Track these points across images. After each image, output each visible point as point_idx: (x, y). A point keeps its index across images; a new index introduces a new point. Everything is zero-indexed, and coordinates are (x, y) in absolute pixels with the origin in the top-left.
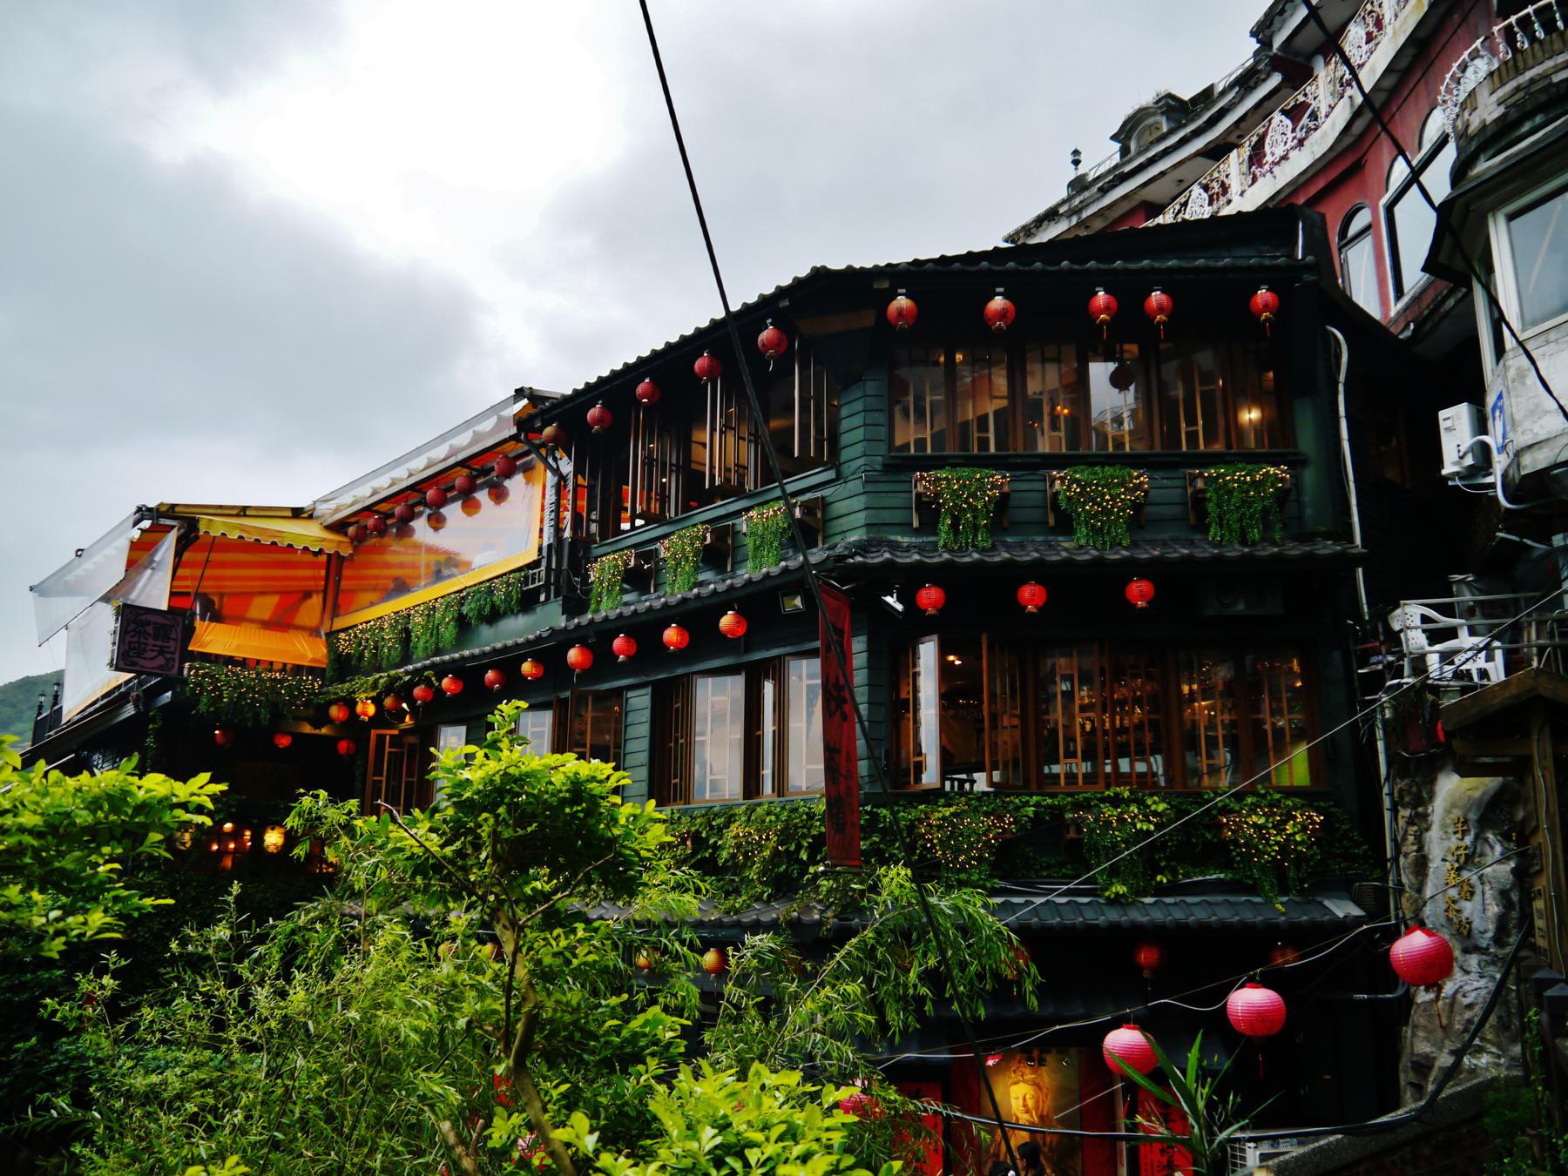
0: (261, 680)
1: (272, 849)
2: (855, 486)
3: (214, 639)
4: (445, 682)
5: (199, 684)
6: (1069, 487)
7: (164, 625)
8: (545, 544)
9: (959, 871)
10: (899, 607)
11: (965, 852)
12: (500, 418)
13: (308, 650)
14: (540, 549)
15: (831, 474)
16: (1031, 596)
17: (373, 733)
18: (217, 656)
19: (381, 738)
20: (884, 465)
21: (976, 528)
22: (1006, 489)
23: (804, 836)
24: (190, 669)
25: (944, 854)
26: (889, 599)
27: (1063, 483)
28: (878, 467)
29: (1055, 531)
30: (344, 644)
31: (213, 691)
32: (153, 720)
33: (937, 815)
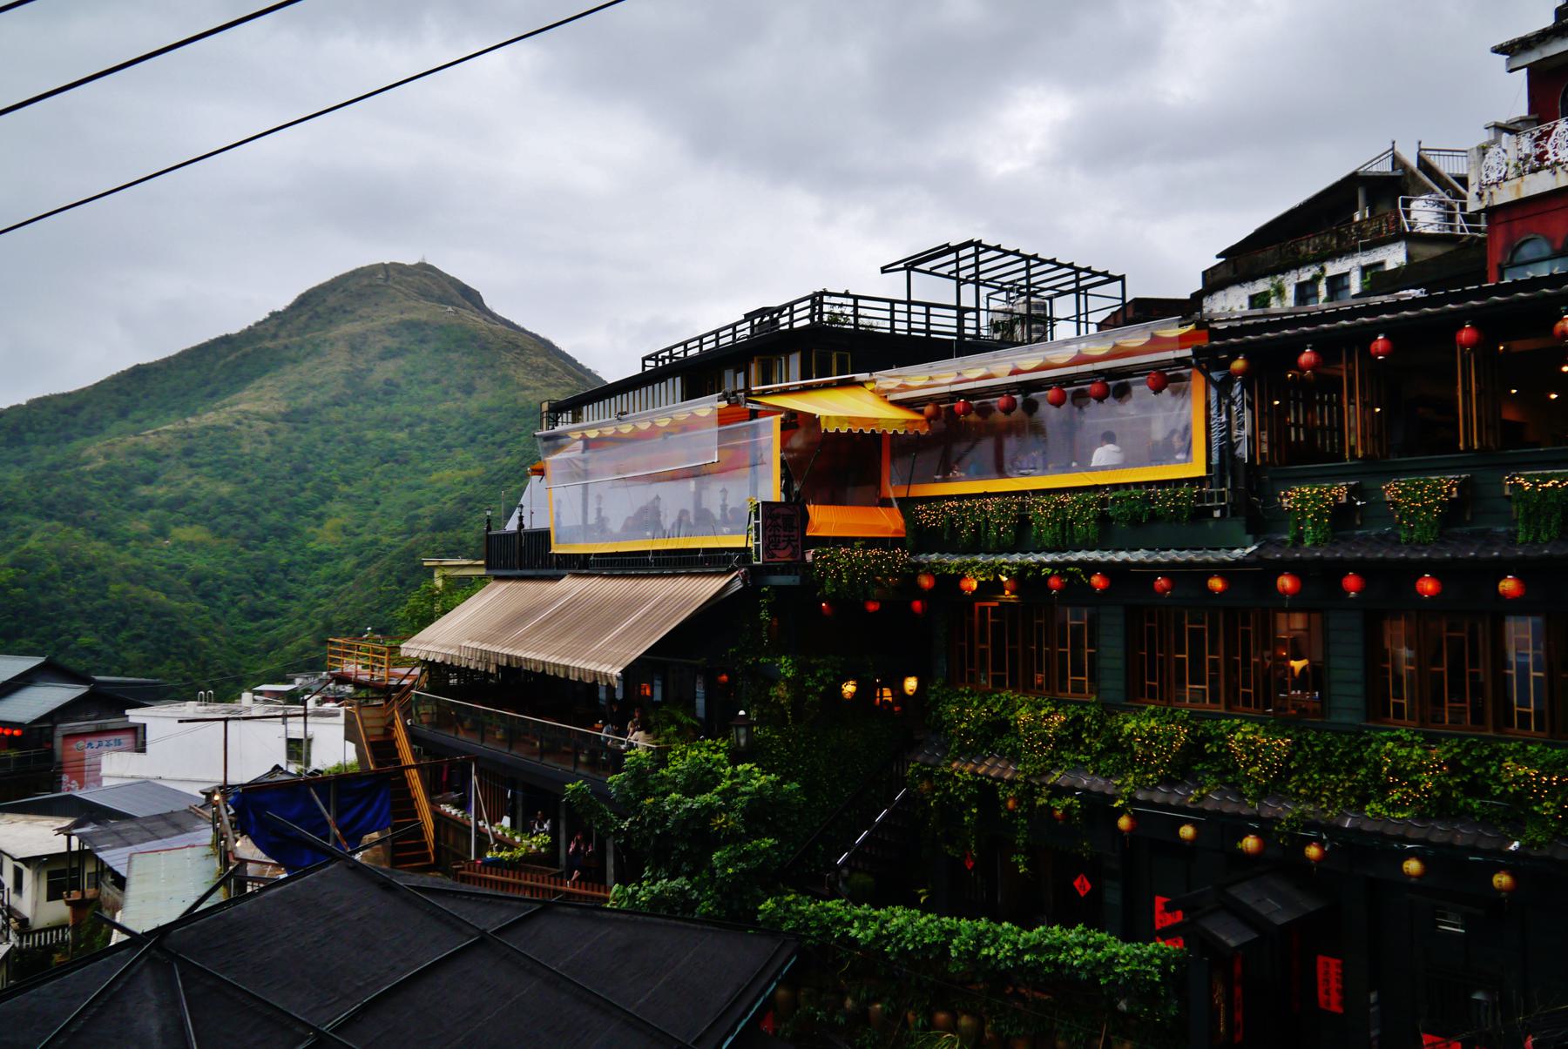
0: (867, 558)
1: (848, 696)
12: (1153, 336)
14: (1209, 467)
17: (977, 605)
24: (814, 556)
30: (926, 516)
32: (764, 595)
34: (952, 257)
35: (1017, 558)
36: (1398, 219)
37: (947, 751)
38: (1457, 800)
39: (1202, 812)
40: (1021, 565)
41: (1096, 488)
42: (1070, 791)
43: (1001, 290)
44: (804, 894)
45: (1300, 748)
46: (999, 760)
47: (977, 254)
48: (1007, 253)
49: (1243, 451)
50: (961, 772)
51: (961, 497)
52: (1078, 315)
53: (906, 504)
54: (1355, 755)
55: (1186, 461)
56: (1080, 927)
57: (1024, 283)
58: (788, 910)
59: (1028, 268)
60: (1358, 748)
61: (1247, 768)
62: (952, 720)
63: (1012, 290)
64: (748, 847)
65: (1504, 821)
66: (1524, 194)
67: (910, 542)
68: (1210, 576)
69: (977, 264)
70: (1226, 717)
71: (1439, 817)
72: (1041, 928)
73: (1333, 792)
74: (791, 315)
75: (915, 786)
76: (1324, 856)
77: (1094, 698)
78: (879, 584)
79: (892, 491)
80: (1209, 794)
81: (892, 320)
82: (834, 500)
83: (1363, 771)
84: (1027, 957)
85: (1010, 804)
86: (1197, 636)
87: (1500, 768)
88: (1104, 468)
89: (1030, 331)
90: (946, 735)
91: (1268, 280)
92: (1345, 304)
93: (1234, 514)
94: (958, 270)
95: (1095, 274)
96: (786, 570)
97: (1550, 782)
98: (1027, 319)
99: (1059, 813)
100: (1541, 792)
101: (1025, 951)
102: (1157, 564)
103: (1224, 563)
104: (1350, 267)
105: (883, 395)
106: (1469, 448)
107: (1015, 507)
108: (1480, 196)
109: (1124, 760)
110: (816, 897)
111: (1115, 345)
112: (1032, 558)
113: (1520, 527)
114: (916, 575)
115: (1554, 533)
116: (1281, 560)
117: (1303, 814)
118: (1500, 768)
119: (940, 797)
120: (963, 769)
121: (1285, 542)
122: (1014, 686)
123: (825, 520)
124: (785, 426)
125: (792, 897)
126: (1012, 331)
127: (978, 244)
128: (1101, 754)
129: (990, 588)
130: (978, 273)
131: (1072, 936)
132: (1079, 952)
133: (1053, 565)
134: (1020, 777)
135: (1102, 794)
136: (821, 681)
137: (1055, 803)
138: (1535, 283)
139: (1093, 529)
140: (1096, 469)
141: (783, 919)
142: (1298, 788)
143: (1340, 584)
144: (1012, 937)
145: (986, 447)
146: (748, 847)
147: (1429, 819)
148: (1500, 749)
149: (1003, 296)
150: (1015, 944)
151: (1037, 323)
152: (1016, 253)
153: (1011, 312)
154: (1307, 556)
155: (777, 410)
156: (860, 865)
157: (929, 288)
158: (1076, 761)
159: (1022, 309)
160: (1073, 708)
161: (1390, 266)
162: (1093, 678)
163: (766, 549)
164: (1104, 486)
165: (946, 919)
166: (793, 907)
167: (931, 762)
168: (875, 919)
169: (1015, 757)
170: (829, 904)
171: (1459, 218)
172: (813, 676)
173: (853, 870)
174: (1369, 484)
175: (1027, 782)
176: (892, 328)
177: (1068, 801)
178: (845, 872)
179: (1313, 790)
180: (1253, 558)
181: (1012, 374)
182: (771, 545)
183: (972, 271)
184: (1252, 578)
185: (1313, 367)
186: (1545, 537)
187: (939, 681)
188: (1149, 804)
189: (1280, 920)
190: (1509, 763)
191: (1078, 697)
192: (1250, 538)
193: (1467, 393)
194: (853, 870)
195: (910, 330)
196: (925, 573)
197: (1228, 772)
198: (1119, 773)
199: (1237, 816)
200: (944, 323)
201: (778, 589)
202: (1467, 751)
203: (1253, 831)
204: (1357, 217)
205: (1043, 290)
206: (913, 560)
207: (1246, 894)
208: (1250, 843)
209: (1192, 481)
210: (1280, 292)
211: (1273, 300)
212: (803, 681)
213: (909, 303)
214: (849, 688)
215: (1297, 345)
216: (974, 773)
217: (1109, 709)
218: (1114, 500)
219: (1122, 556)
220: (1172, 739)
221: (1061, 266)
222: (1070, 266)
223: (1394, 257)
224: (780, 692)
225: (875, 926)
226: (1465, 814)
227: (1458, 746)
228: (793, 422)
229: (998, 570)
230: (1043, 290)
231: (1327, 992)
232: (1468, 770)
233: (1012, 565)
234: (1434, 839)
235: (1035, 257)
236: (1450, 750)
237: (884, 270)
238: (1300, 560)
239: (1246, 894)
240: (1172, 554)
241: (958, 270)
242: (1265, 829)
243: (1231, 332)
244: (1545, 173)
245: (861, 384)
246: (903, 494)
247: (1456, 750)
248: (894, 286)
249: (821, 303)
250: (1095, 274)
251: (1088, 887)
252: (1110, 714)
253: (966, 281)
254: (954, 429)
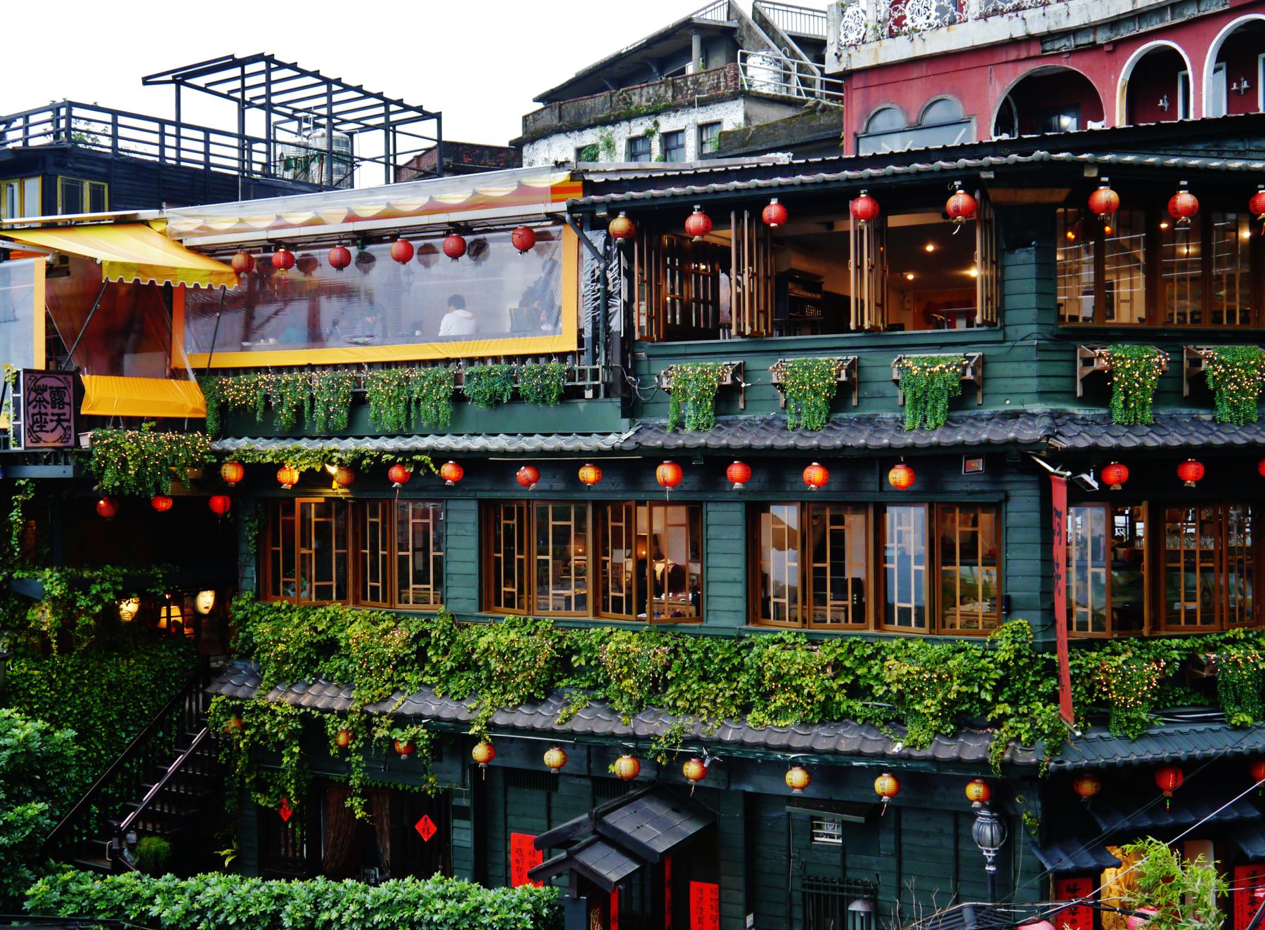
0: (160, 444)
7: (58, 388)
8: (588, 334)
10: (1095, 485)
12: (520, 185)
14: (581, 342)
17: (298, 501)
18: (117, 418)
19: (305, 507)
21: (1144, 405)
23: (986, 680)
24: (93, 440)
26: (1085, 477)
30: (233, 391)
32: (20, 490)
34: (236, 72)
35: (350, 444)
36: (736, 76)
37: (260, 680)
38: (840, 703)
39: (572, 734)
40: (356, 452)
41: (447, 361)
42: (417, 719)
43: (292, 118)
44: (84, 868)
45: (677, 656)
46: (326, 687)
47: (268, 72)
48: (304, 73)
49: (617, 324)
50: (279, 704)
51: (279, 369)
52: (387, 155)
53: (203, 374)
54: (736, 661)
55: (554, 333)
56: (437, 876)
57: (324, 111)
58: (65, 891)
59: (329, 94)
60: (738, 653)
61: (619, 680)
62: (266, 641)
63: (306, 120)
64: (10, 816)
65: (886, 722)
66: (881, 61)
67: (212, 425)
68: (581, 464)
69: (269, 83)
70: (596, 624)
71: (822, 722)
72: (392, 882)
73: (714, 702)
74: (26, 129)
75: (217, 725)
76: (705, 773)
77: (442, 609)
78: (175, 478)
79: (187, 356)
80: (578, 714)
81: (162, 146)
82: (115, 369)
83: (744, 678)
84: (377, 918)
85: (342, 739)
86: (562, 536)
87: (882, 668)
88: (456, 339)
89: (330, 171)
90: (257, 661)
91: (597, 131)
92: (673, 167)
93: (607, 395)
94: (243, 89)
95: (407, 108)
96: (55, 457)
97: (931, 679)
98: (328, 156)
99: (402, 746)
100: (921, 689)
101: (376, 910)
102: (524, 453)
103: (601, 452)
104: (685, 121)
105: (178, 240)
106: (860, 329)
107: (348, 383)
108: (838, 57)
109: (478, 679)
110: (101, 873)
111: (475, 193)
112: (369, 445)
113: (908, 413)
114: (220, 464)
115: (941, 420)
116: (662, 449)
117: (682, 729)
118: (882, 668)
119: (253, 736)
120: (283, 700)
121: (664, 427)
122: (342, 596)
123: (104, 394)
124: (51, 271)
125: (68, 876)
126: (306, 170)
127: (269, 59)
128: (451, 672)
129: (314, 479)
130: (269, 94)
131: (430, 886)
132: (439, 904)
133: (399, 453)
134: (356, 706)
135: (456, 721)
136: (98, 599)
137: (397, 734)
138: (892, 158)
139: (445, 409)
140: (447, 339)
141: (59, 904)
142: (675, 700)
143: (725, 475)
144: (358, 896)
145: (298, 311)
146: (10, 816)
147: (812, 724)
148: (882, 647)
149: (294, 126)
150: (362, 904)
151: (341, 162)
152: (316, 74)
153: (307, 147)
154: (691, 443)
155: (41, 251)
156: (149, 827)
157: (208, 110)
158: (421, 684)
159: (321, 144)
160: (416, 622)
161: (727, 127)
162: (438, 583)
163: (30, 431)
164: (458, 360)
165: (273, 882)
166: (73, 887)
167: (240, 693)
168: (183, 891)
169: (346, 682)
170: (121, 879)
171: (795, 79)
172: (86, 593)
173: (141, 834)
174: (754, 363)
175: (362, 712)
176: (162, 156)
177: (414, 731)
178: (132, 837)
179: (691, 702)
180: (631, 445)
181: (351, 218)
182: (36, 425)
183: (262, 91)
184: (631, 467)
185: (703, 232)
186: (932, 424)
187: (248, 595)
188: (512, 728)
189: (661, 846)
190: (891, 661)
191: (421, 608)
192: (627, 421)
193: (859, 267)
194: (141, 834)
195: (179, 159)
196: (232, 463)
197: (597, 686)
198: (473, 694)
199: (612, 736)
200: (225, 157)
201: (40, 483)
202: (850, 651)
203: (627, 751)
204: (690, 69)
205: (344, 122)
206: (216, 446)
207: (623, 821)
208: (624, 766)
209: (562, 356)
210: (610, 145)
211: (602, 155)
212: (72, 603)
213: (178, 124)
214: (129, 608)
215: (682, 209)
216: (297, 706)
217: (459, 621)
218: (469, 377)
219: (478, 443)
220: (535, 653)
221: (368, 95)
222: (379, 96)
223: (732, 116)
224: (44, 616)
225: (185, 900)
226: (847, 717)
227: (841, 646)
228: (60, 265)
229: (327, 458)
230: (344, 122)
231: (700, 920)
232: (849, 671)
233: (345, 452)
234: (819, 746)
235: (338, 81)
236: (833, 651)
237: (146, 81)
238: (683, 448)
239: (623, 821)
240: (537, 442)
241: (243, 89)
242: (638, 746)
243: (608, 186)
244: (902, 40)
245: (146, 223)
246: (203, 364)
247: (840, 651)
248: (160, 101)
249: (69, 117)
250: (407, 108)
251: (434, 829)
252: (462, 627)
253: (250, 105)
254: (263, 280)
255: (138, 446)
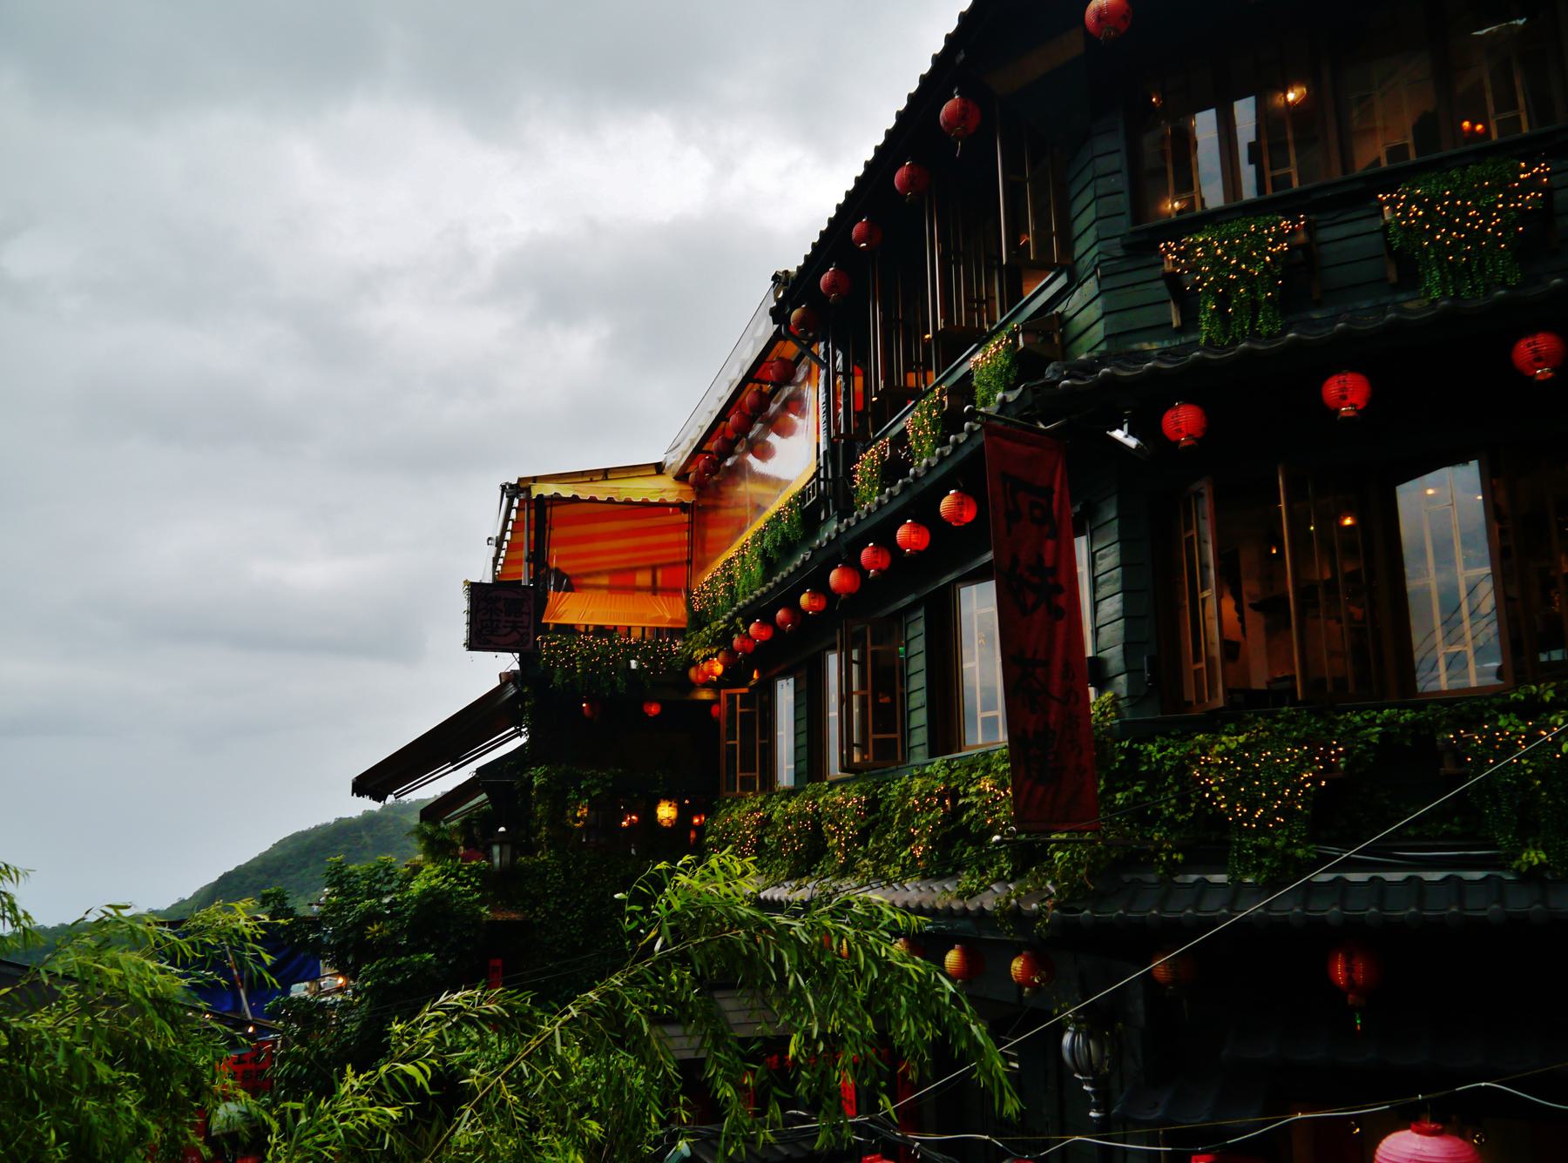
1: (666, 823)
2: (1090, 287)
3: (571, 610)
4: (752, 627)
5: (552, 657)
6: (1405, 210)
9: (1256, 834)
10: (1132, 442)
11: (1265, 804)
13: (667, 612)
15: (1062, 281)
16: (1345, 393)
19: (731, 698)
20: (1124, 247)
22: (1302, 237)
25: (1232, 807)
26: (1118, 434)
27: (1394, 210)
28: (1119, 253)
29: (1397, 288)
31: (566, 662)
33: (1218, 748)
172: (578, 789)
255: (591, 648)
